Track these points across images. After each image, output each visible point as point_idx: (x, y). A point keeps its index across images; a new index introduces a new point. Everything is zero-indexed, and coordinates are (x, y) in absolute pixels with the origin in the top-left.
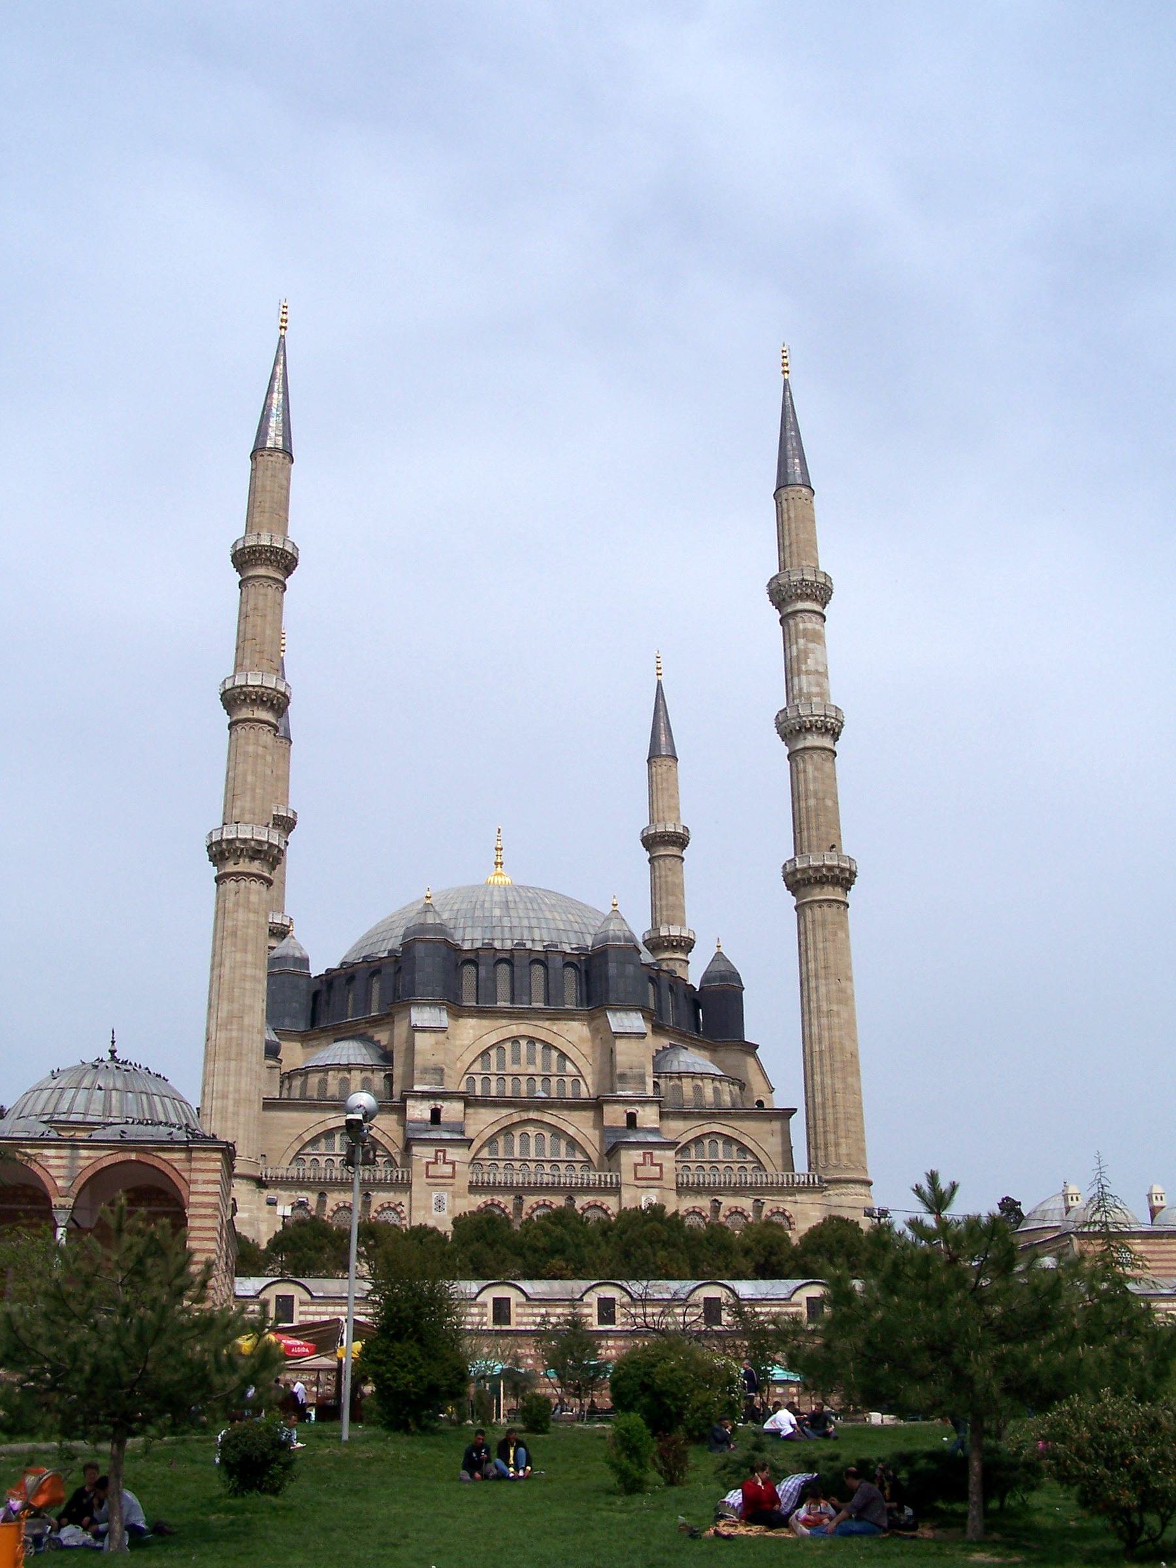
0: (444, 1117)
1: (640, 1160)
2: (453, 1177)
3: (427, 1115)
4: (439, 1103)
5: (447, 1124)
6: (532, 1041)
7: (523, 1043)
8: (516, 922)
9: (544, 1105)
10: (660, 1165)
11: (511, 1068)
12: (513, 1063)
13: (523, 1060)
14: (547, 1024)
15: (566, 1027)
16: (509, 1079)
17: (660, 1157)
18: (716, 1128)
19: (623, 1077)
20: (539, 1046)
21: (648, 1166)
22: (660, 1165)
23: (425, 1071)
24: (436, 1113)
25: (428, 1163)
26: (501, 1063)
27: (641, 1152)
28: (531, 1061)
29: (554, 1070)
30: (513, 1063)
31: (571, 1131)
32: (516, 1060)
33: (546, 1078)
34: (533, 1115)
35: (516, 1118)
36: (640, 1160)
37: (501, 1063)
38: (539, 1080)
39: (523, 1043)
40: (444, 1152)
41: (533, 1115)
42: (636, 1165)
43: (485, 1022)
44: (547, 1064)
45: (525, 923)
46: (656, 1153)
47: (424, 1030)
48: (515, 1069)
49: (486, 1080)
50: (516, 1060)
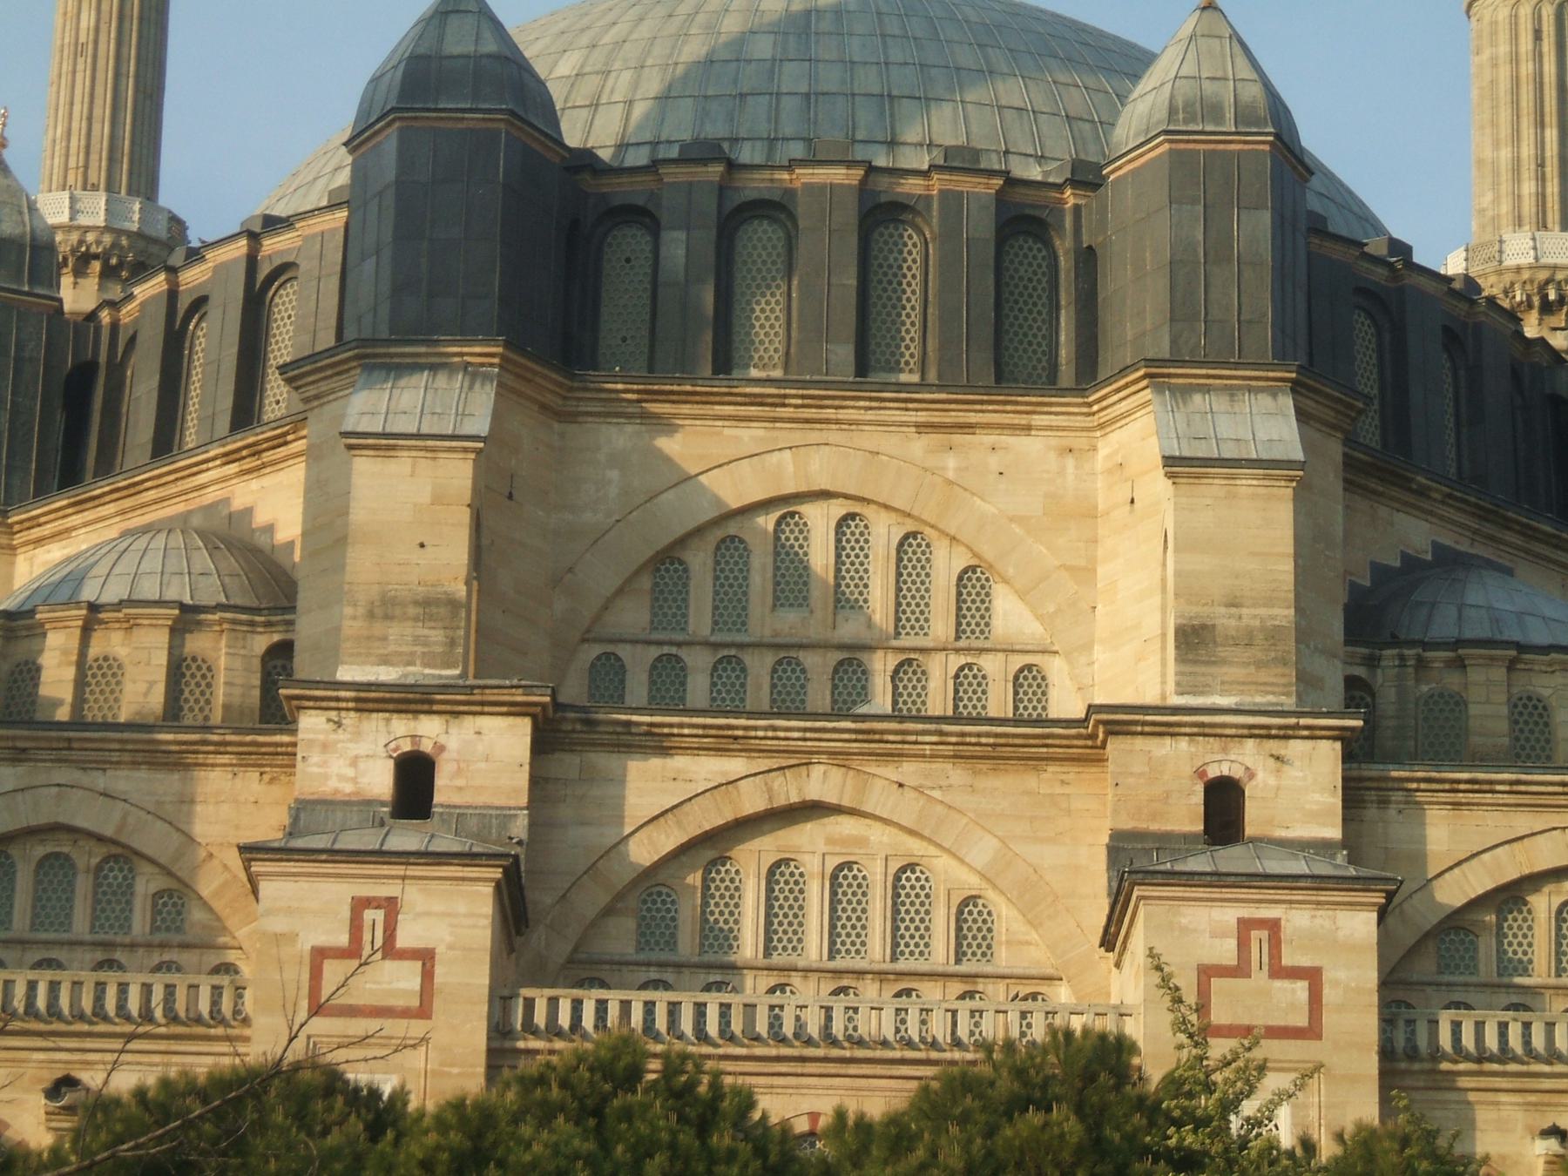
0: (446, 789)
1: (1226, 951)
2: (423, 1011)
3: (380, 781)
4: (429, 730)
5: (459, 818)
8: (831, 79)
10: (1313, 976)
12: (778, 602)
14: (918, 446)
15: (994, 462)
21: (1260, 977)
22: (1313, 976)
23: (385, 608)
24: (415, 778)
25: (320, 955)
27: (1229, 915)
29: (941, 627)
30: (778, 602)
35: (752, 801)
36: (1226, 951)
40: (391, 907)
45: (869, 81)
47: (385, 443)
48: (788, 622)
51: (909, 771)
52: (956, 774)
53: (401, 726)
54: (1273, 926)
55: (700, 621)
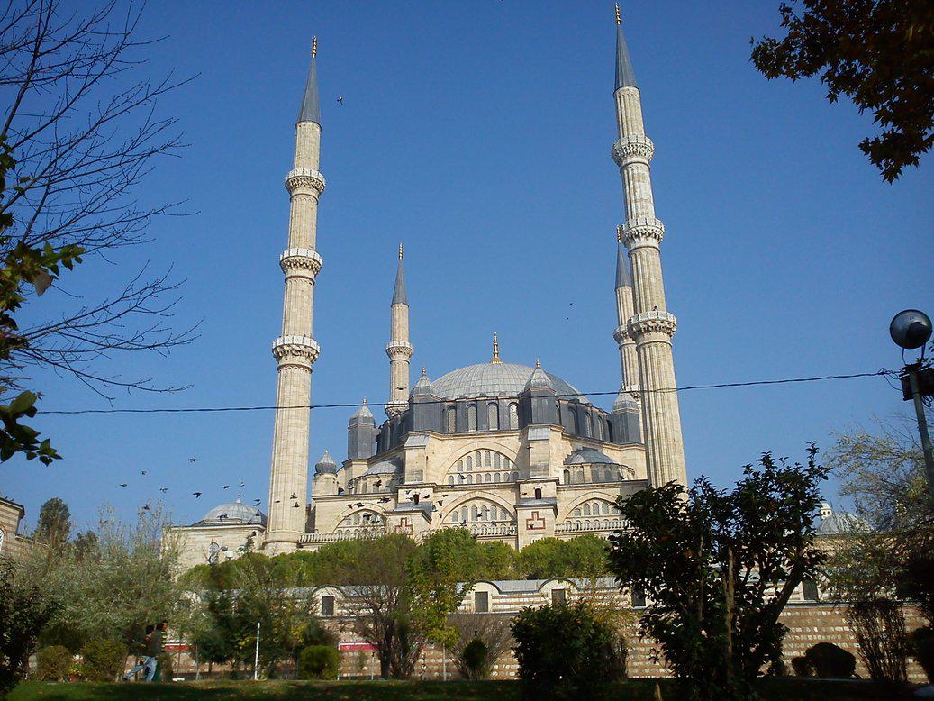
6: (488, 450)
7: (483, 452)
9: (485, 487)
10: (544, 519)
11: (475, 469)
13: (483, 462)
16: (474, 475)
17: (543, 514)
18: (597, 495)
19: (535, 467)
22: (544, 519)
26: (470, 467)
27: (531, 511)
29: (502, 468)
31: (502, 503)
33: (498, 474)
34: (478, 494)
37: (470, 467)
38: (492, 474)
41: (478, 494)
42: (527, 520)
43: (458, 442)
44: (497, 465)
46: (540, 511)
48: (478, 469)
51: (491, 491)
52: (498, 491)
53: (413, 490)
54: (537, 512)
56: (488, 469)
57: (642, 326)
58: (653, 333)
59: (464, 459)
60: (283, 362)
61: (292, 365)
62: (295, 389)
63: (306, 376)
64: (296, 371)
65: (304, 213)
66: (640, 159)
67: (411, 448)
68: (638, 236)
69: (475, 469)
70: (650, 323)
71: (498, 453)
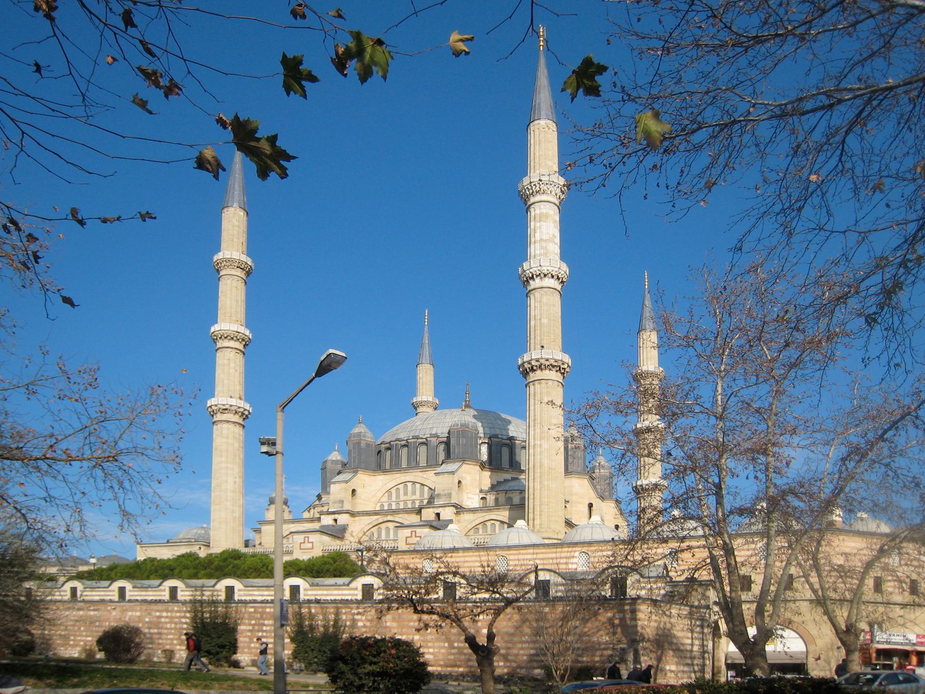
6: (414, 483)
7: (409, 485)
14: (421, 474)
20: (418, 486)
26: (398, 496)
28: (414, 493)
32: (406, 494)
37: (398, 496)
39: (409, 485)
48: (405, 498)
49: (390, 505)
50: (406, 494)
55: (394, 498)
56: (414, 497)
57: (526, 365)
58: (539, 372)
59: (393, 491)
60: (215, 419)
61: (221, 421)
62: (224, 440)
63: (238, 430)
64: (225, 425)
65: (231, 294)
66: (544, 197)
67: (335, 483)
68: (532, 278)
69: (402, 497)
70: (533, 363)
71: (423, 485)
